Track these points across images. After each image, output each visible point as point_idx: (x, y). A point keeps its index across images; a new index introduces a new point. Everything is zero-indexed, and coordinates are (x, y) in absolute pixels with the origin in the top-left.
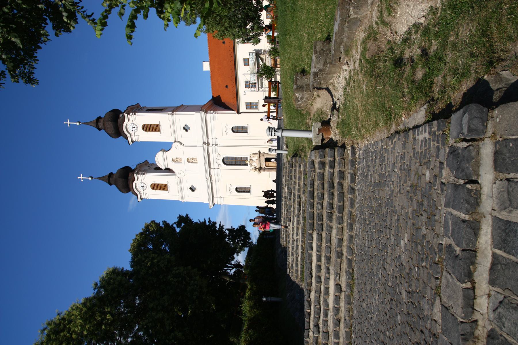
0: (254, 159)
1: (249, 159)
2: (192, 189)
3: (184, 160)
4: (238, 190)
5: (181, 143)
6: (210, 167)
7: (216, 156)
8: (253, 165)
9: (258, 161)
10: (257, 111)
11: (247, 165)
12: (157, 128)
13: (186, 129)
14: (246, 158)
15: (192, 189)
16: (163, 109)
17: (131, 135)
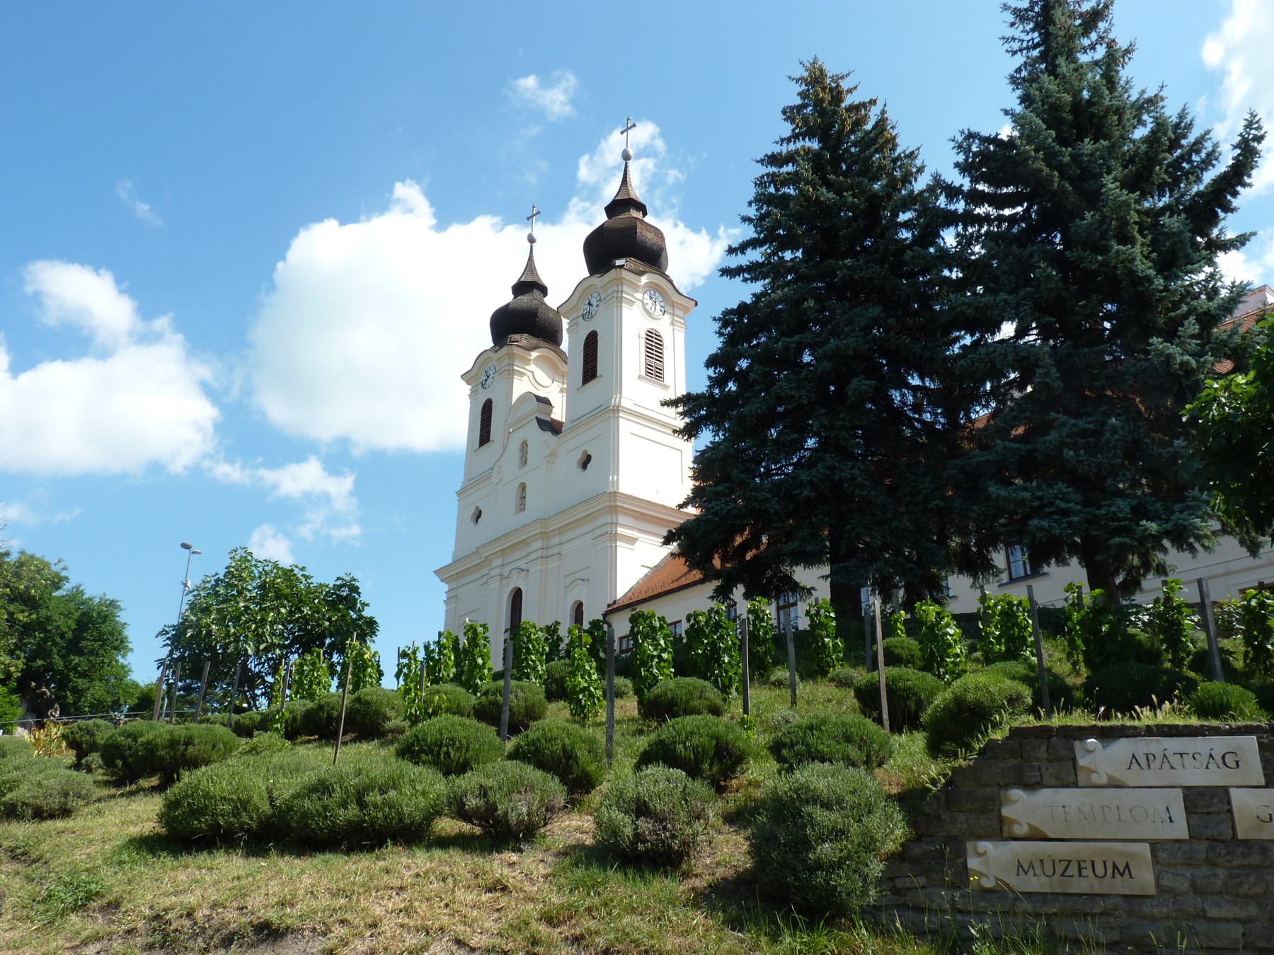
6: (503, 552)
7: (521, 564)
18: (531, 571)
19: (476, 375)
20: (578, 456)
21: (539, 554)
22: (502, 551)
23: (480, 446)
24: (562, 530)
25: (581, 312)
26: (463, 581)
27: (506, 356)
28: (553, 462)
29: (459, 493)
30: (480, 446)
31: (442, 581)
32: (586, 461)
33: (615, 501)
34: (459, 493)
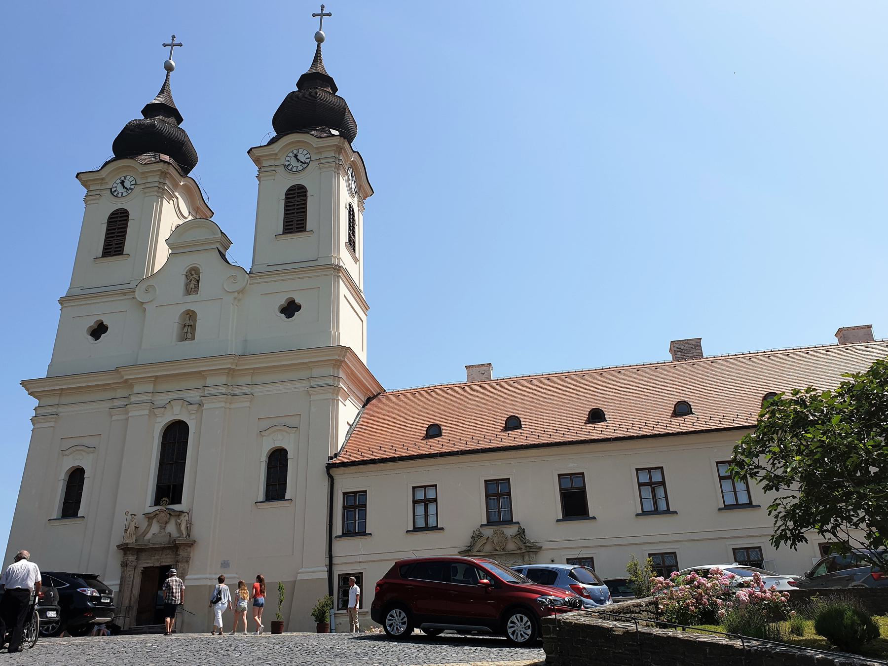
0: (171, 528)
1: (176, 507)
2: (98, 331)
3: (192, 303)
4: (76, 477)
5: (241, 291)
7: (194, 396)
8: (150, 525)
9: (162, 540)
10: (338, 530)
11: (157, 502)
12: (295, 226)
13: (290, 309)
14: (177, 500)
15: (98, 331)
16: (354, 250)
17: (276, 154)
18: (206, 406)
19: (102, 179)
20: (282, 301)
21: (223, 390)
22: (156, 377)
23: (103, 256)
24: (255, 371)
25: (282, 162)
26: (64, 400)
27: (159, 173)
28: (239, 300)
29: (62, 301)
30: (103, 256)
31: (31, 394)
32: (290, 309)
33: (344, 357)
34: (62, 301)
